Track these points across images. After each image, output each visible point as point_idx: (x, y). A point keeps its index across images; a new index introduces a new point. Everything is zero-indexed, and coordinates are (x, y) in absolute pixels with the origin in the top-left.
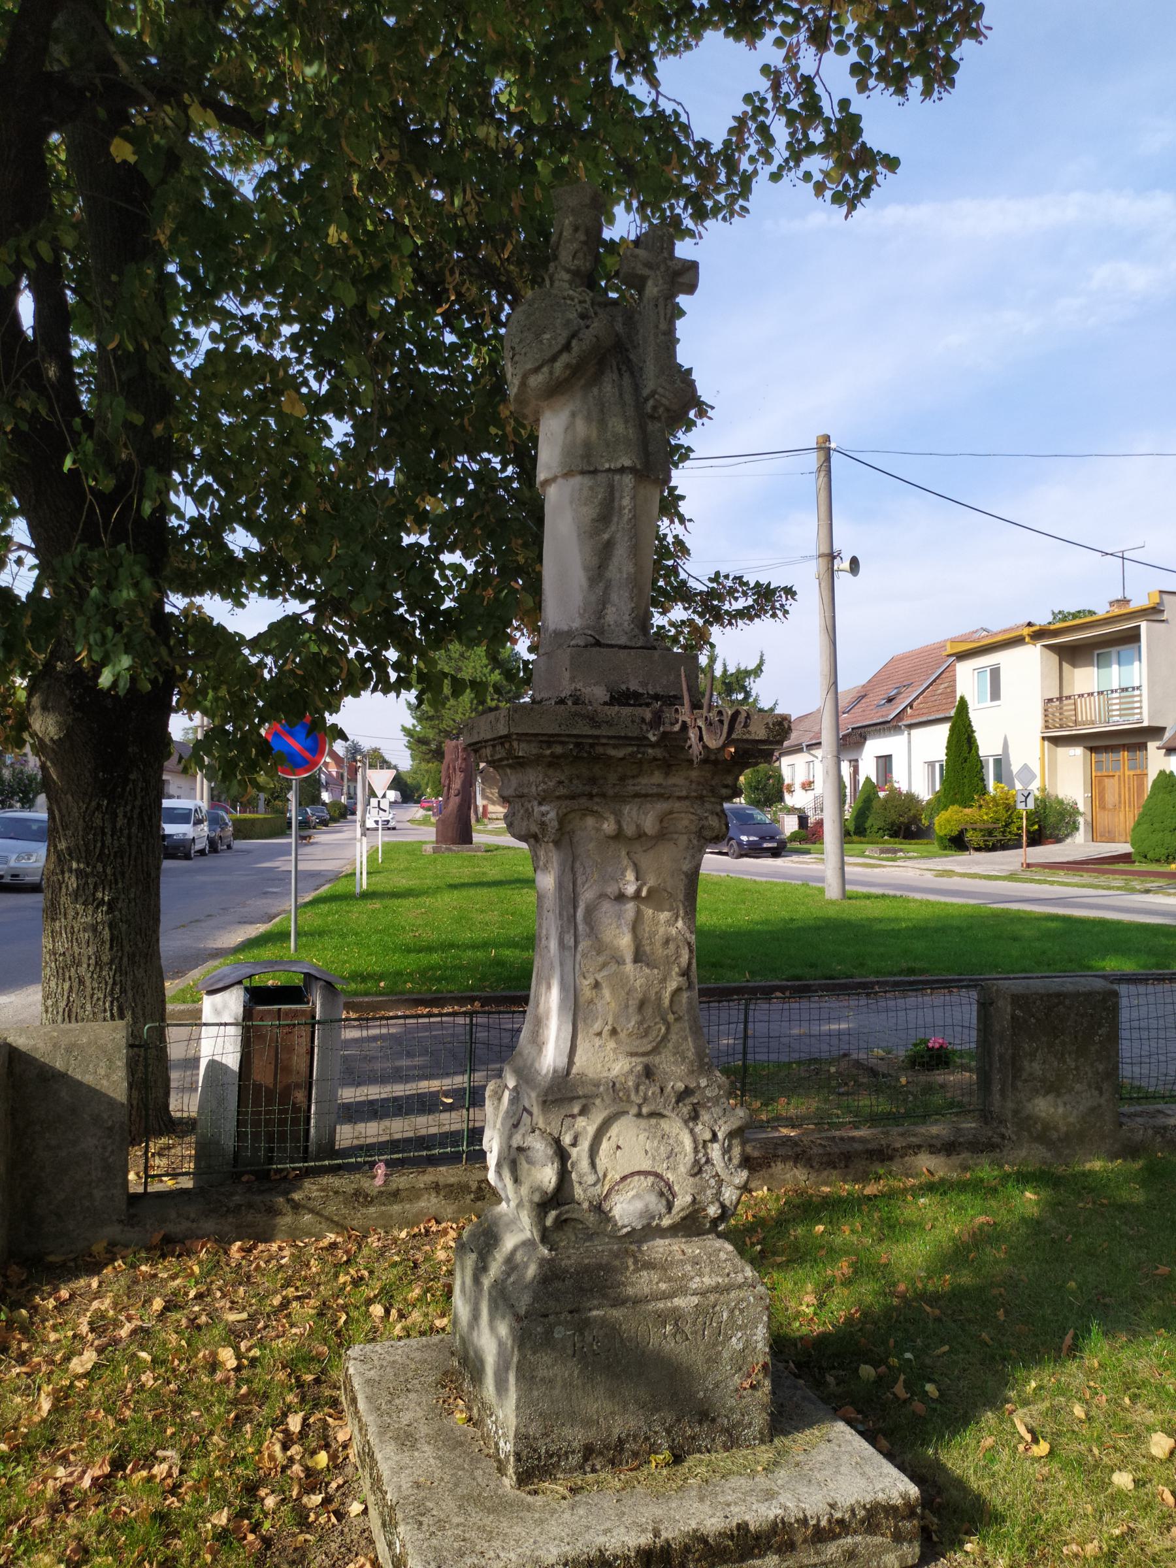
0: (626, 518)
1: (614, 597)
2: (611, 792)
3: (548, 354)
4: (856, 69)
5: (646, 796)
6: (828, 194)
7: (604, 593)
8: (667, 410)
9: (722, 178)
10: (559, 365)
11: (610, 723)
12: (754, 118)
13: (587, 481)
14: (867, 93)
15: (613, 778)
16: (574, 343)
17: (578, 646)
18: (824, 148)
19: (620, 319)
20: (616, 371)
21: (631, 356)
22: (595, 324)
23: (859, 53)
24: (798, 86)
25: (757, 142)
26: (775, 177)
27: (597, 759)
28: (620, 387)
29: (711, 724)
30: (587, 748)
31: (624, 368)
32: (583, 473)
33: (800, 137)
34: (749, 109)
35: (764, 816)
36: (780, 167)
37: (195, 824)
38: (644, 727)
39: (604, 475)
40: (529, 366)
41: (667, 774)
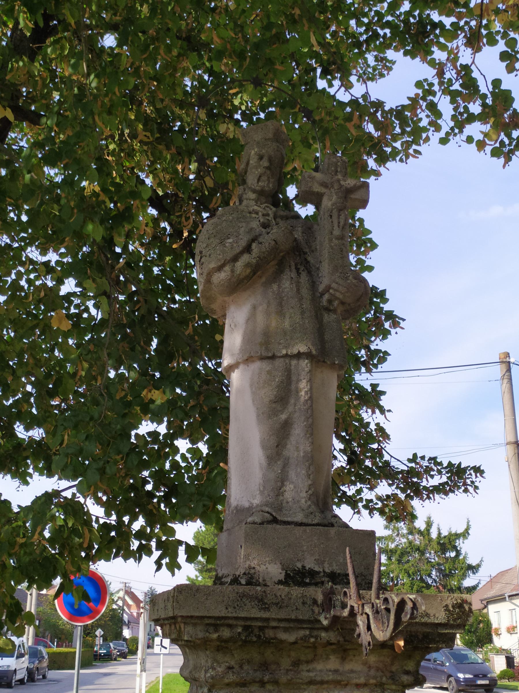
0: (302, 399)
1: (292, 474)
2: (284, 679)
3: (229, 255)
4: (504, 56)
5: (322, 683)
6: (488, 149)
7: (282, 471)
8: (343, 303)
9: (398, 130)
10: (239, 265)
11: (279, 605)
12: (424, 99)
13: (265, 366)
14: (515, 73)
15: (286, 663)
16: (254, 245)
17: (254, 523)
18: (482, 118)
19: (300, 229)
20: (294, 270)
21: (309, 259)
22: (275, 231)
23: (506, 44)
24: (458, 73)
25: (427, 116)
26: (444, 141)
27: (268, 642)
28: (298, 282)
29: (377, 612)
30: (256, 631)
31: (302, 268)
32: (262, 358)
33: (462, 110)
34: (420, 92)
35: (478, 656)
36: (447, 134)
37: (18, 658)
38: (316, 609)
39: (282, 359)
40: (212, 265)
41: (343, 659)
